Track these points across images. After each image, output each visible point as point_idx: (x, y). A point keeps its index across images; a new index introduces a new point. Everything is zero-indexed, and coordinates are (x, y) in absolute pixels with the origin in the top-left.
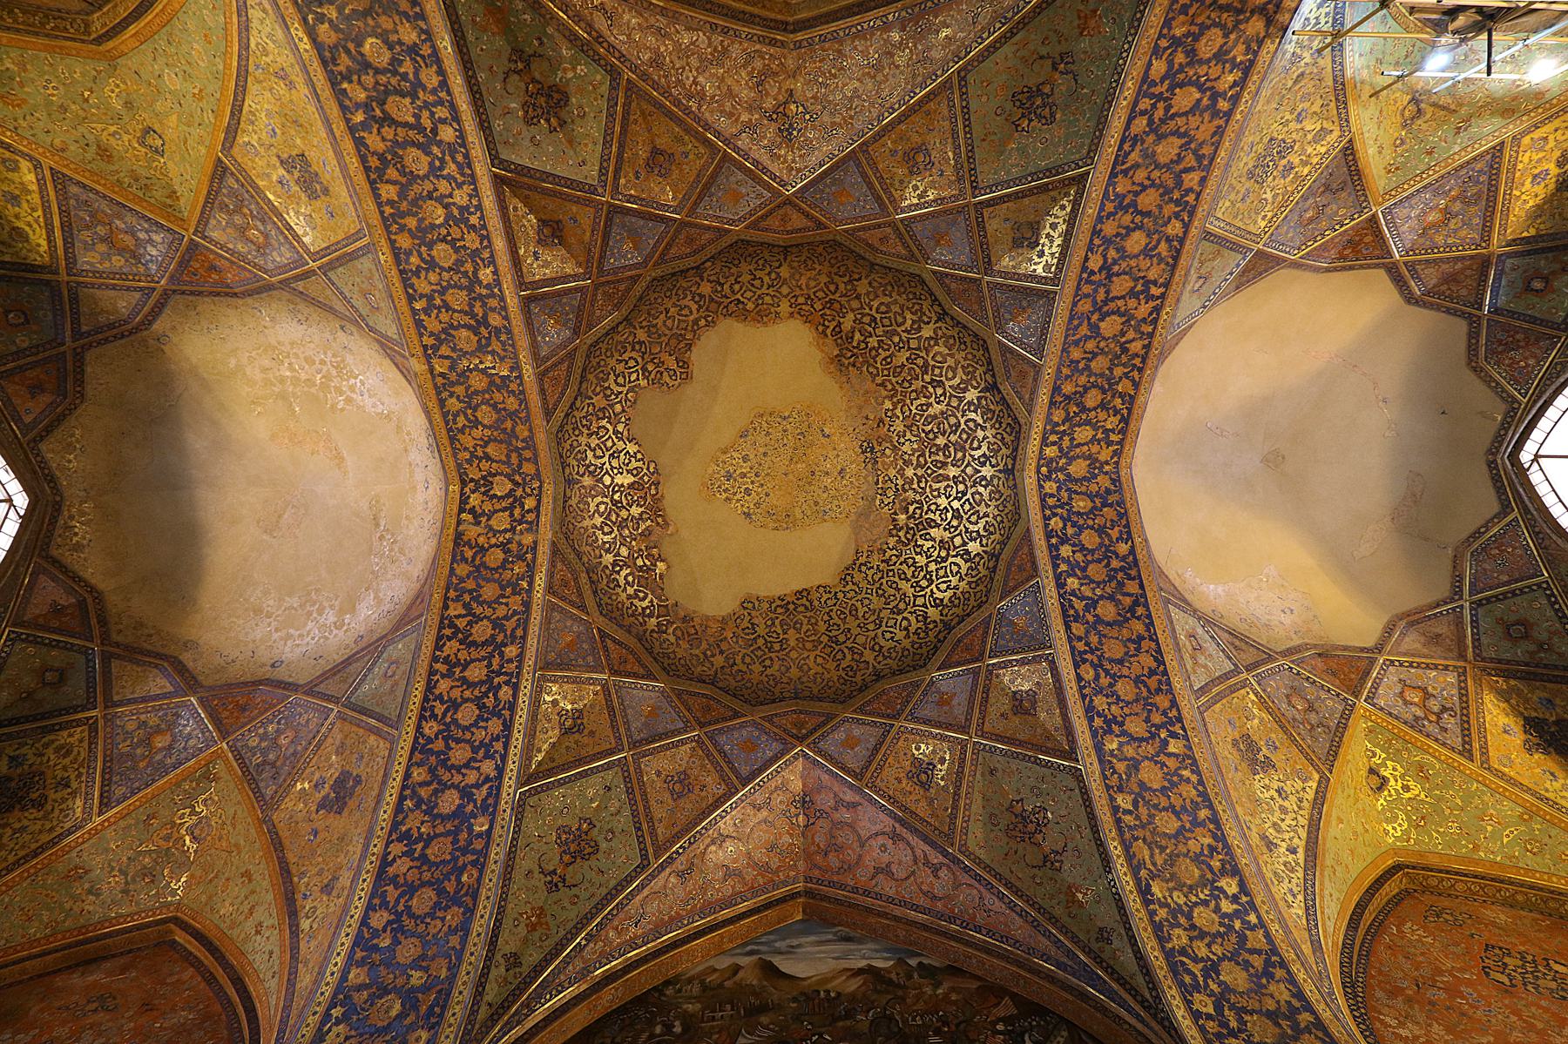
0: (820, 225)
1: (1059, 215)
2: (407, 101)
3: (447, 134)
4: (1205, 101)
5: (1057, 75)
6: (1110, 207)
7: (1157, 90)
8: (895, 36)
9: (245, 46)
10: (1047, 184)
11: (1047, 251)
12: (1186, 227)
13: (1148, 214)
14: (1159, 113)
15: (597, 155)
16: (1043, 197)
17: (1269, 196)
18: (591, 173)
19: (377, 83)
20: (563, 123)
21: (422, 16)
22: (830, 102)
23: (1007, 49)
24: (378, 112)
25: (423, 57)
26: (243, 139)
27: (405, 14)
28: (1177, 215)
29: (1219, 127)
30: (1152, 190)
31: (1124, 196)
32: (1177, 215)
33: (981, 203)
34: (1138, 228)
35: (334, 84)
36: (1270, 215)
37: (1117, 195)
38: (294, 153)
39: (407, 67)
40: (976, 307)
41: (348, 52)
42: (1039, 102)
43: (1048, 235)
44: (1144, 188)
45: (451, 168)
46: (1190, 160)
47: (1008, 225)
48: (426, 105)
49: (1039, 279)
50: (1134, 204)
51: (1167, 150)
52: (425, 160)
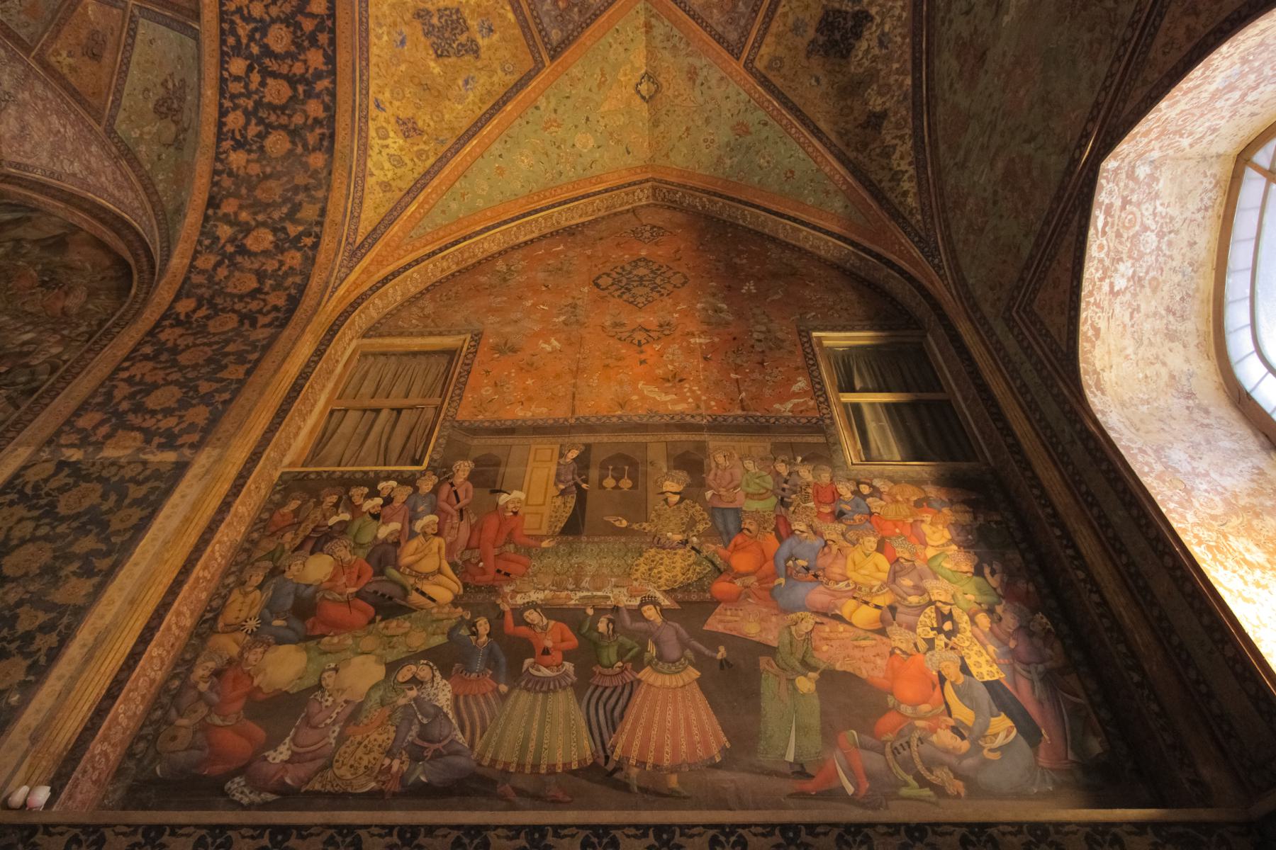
2: (266, 100)
3: (237, 66)
9: (442, 161)
15: (137, 50)
18: (146, 29)
19: (290, 116)
20: (164, 84)
21: (216, 172)
24: (301, 89)
25: (233, 138)
26: (511, 79)
27: (230, 174)
35: (332, 118)
38: (453, 59)
39: (253, 130)
41: (305, 146)
45: (243, 30)
48: (248, 95)
52: (270, 40)
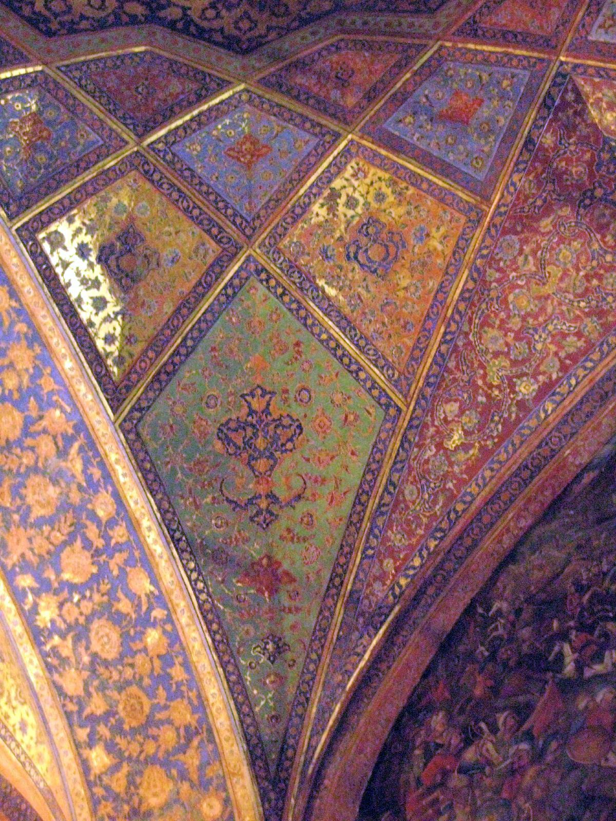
0: (472, 31)
1: (106, 328)
4: (51, 575)
5: (262, 489)
6: (47, 384)
7: (119, 558)
8: (526, 389)
10: (158, 354)
11: (79, 263)
14: (92, 532)
16: (150, 331)
22: (576, 237)
23: (353, 478)
31: (41, 408)
33: (233, 257)
40: (112, 82)
42: (260, 443)
43: (96, 284)
44: (26, 432)
47: (166, 254)
49: (50, 216)
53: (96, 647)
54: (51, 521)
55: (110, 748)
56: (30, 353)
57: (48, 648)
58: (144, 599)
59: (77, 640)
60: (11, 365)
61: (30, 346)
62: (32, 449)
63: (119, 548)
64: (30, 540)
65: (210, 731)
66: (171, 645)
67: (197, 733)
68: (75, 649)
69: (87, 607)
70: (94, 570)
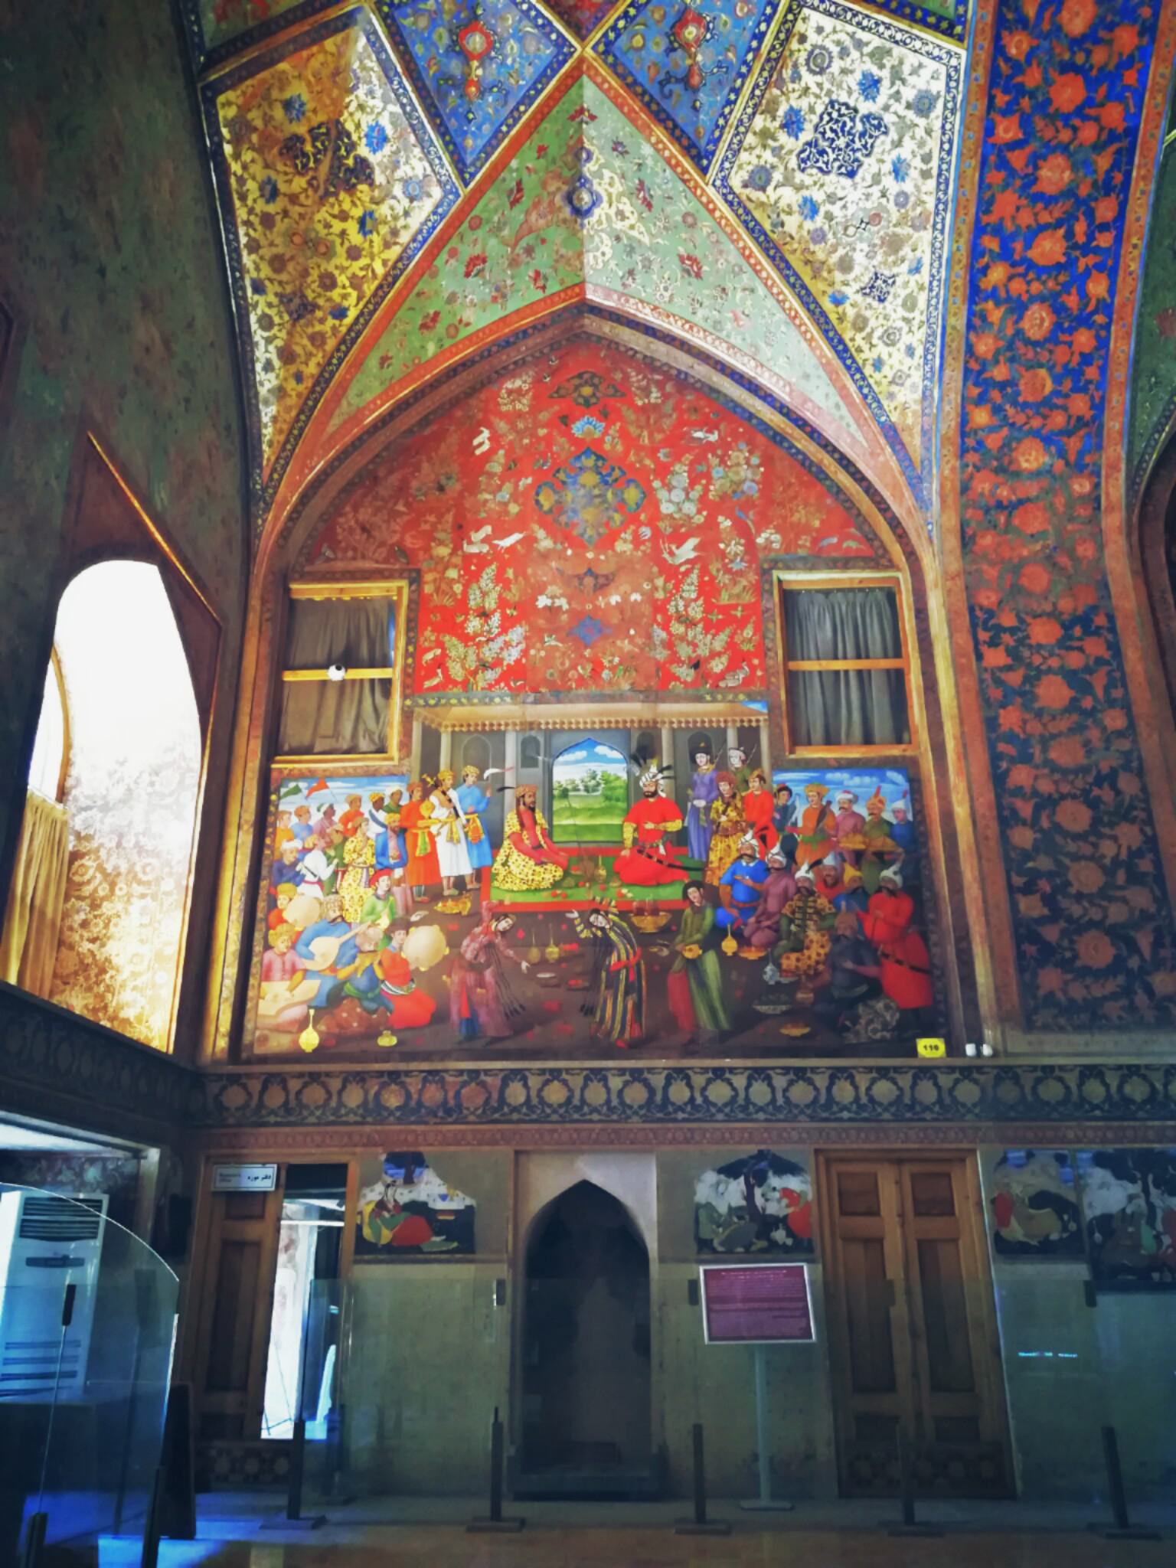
4: (1018, 246)
6: (1130, 77)
12: (998, 49)
13: (1067, 68)
17: (808, 79)
28: (1017, 67)
29: (987, 212)
30: (1068, 108)
31: (1109, 97)
32: (1017, 67)
34: (1077, 42)
36: (794, 45)
37: (1121, 99)
44: (1079, 112)
46: (1018, 159)
50: (1091, 84)
51: (1054, 174)
53: (1025, 325)
54: (1049, 200)
55: (997, 410)
56: (1136, 41)
57: (977, 308)
58: (1093, 302)
59: (1011, 311)
60: (1110, 43)
61: (1141, 34)
62: (1075, 129)
63: (1097, 250)
64: (1018, 209)
65: (1101, 426)
66: (1097, 349)
67: (1087, 425)
68: (1002, 319)
69: (1036, 287)
70: (1063, 260)
